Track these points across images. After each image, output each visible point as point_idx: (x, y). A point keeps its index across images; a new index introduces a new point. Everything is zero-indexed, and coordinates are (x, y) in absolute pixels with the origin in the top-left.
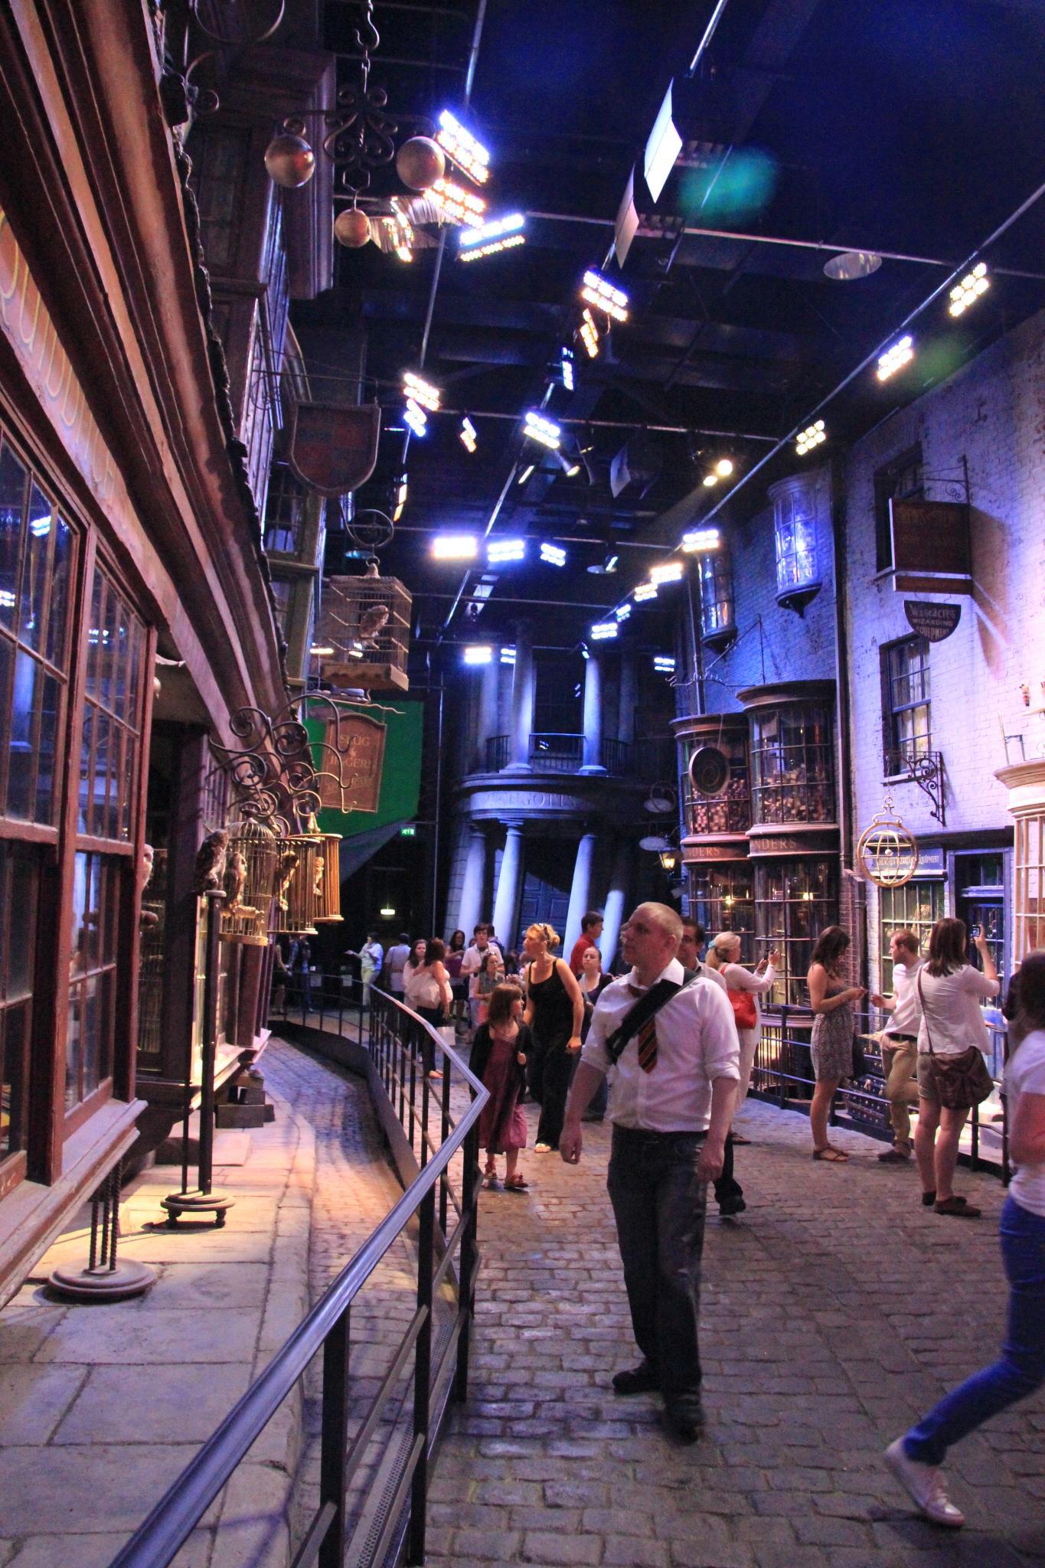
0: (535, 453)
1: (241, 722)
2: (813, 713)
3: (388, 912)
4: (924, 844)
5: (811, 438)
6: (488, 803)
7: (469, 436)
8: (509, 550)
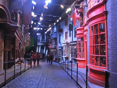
0: (39, 25)
1: (22, 43)
2: (56, 39)
3: (32, 51)
4: (60, 47)
5: (55, 24)
6: (39, 44)
7: (35, 24)
8: (39, 29)
